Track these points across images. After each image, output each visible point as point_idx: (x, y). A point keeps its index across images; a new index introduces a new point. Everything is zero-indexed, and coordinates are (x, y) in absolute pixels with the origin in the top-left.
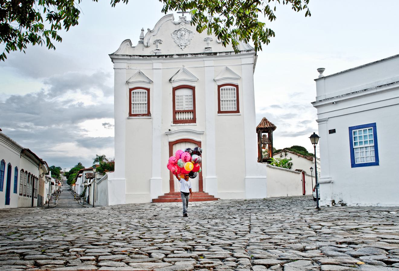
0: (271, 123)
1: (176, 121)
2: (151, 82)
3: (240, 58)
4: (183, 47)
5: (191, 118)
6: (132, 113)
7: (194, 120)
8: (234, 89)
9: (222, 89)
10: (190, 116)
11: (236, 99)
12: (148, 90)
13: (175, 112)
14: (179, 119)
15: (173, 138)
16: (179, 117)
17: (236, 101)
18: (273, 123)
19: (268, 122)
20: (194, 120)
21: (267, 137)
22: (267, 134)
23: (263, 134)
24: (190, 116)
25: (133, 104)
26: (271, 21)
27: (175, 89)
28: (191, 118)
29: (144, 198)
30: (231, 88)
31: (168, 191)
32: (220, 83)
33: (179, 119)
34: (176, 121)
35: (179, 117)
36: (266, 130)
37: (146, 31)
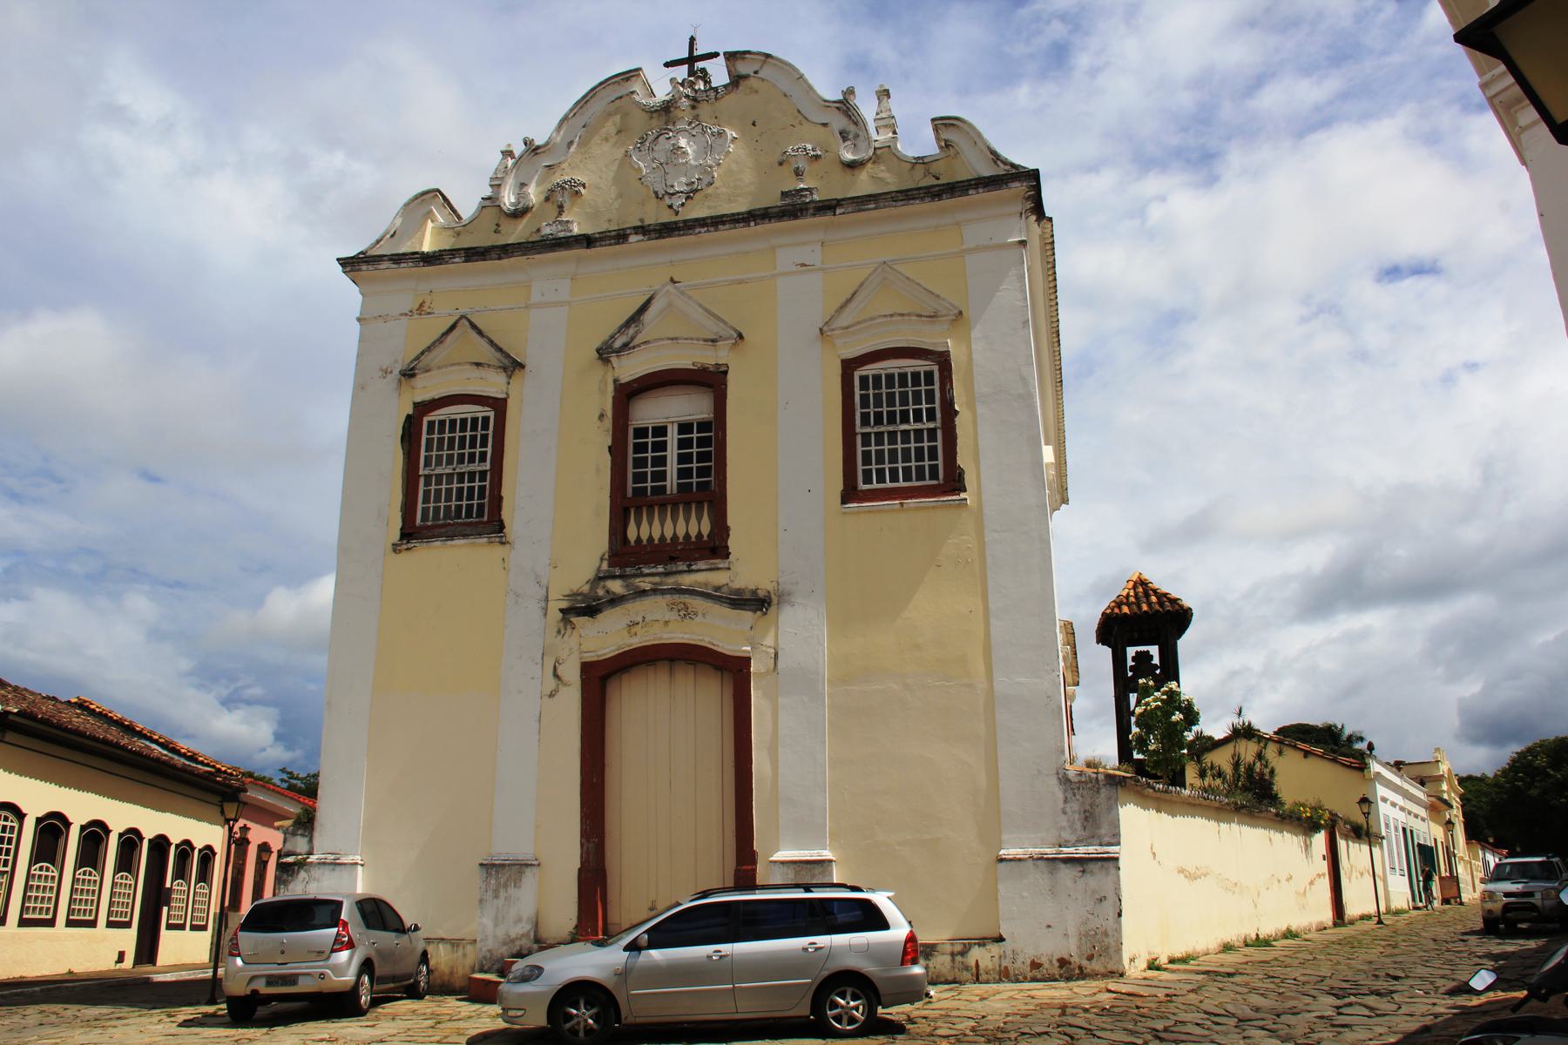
0: (1165, 595)
4: (677, 202)
5: (700, 535)
9: (864, 379)
10: (698, 526)
11: (938, 423)
13: (623, 507)
14: (639, 539)
16: (644, 530)
17: (939, 433)
18: (1174, 594)
19: (1155, 591)
20: (715, 547)
21: (1156, 661)
22: (1154, 650)
23: (1131, 651)
24: (698, 526)
25: (428, 478)
28: (700, 535)
30: (909, 370)
33: (639, 539)
34: (624, 556)
36: (1145, 628)
37: (518, 149)
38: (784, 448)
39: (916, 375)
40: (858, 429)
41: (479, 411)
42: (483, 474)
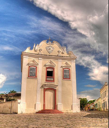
12: (37, 67)
20: (54, 81)
29: (32, 111)
34: (46, 81)
38: (58, 74)
41: (35, 67)
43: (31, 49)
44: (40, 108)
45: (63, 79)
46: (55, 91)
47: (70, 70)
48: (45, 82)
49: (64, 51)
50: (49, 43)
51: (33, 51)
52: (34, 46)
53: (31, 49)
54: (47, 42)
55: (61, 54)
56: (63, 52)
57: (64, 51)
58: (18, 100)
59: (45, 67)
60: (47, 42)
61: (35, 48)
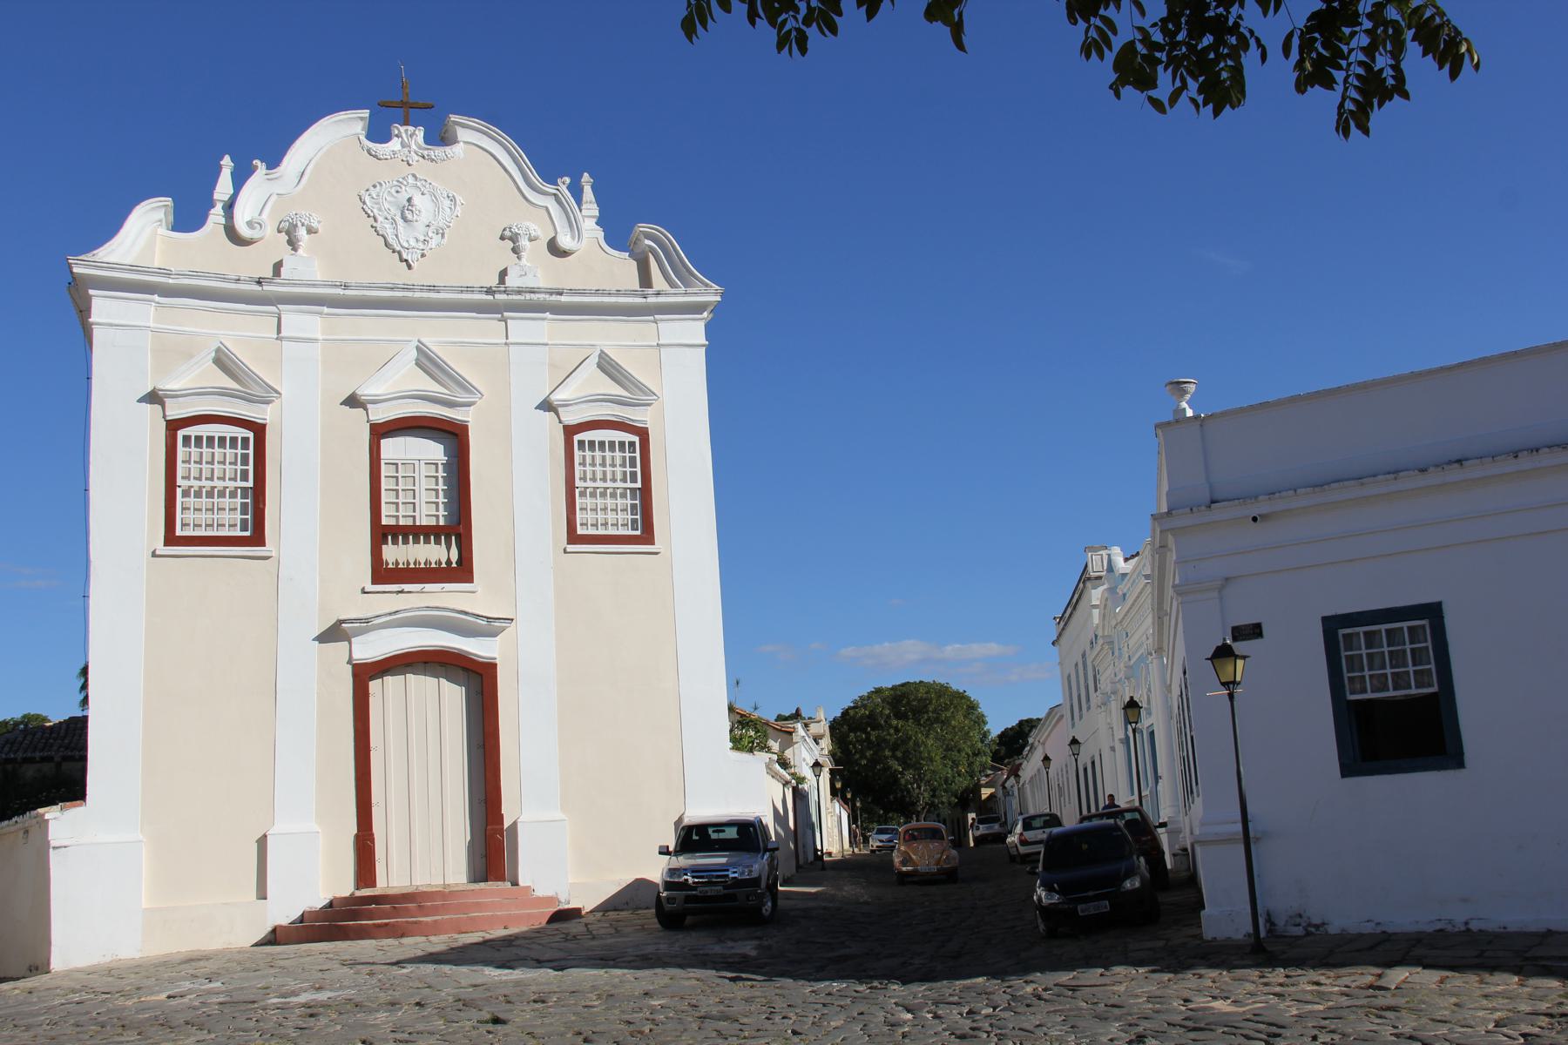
1: (383, 574)
2: (267, 395)
3: (655, 322)
5: (449, 562)
6: (179, 532)
7: (462, 571)
8: (632, 444)
13: (381, 534)
15: (370, 648)
16: (394, 553)
20: (462, 571)
26: (1366, 132)
27: (380, 432)
28: (449, 562)
29: (234, 924)
31: (345, 887)
32: (572, 417)
34: (383, 574)
35: (394, 553)
39: (622, 444)
40: (578, 483)
41: (241, 433)
42: (244, 489)
43: (188, 218)
44: (315, 877)
45: (571, 548)
46: (479, 680)
47: (643, 434)
48: (370, 587)
49: (574, 226)
50: (394, 144)
51: (203, 251)
52: (224, 187)
53: (188, 218)
54: (379, 133)
55: (534, 271)
56: (565, 241)
57: (574, 226)
58: (51, 813)
59: (357, 427)
60: (379, 133)
61: (229, 207)
